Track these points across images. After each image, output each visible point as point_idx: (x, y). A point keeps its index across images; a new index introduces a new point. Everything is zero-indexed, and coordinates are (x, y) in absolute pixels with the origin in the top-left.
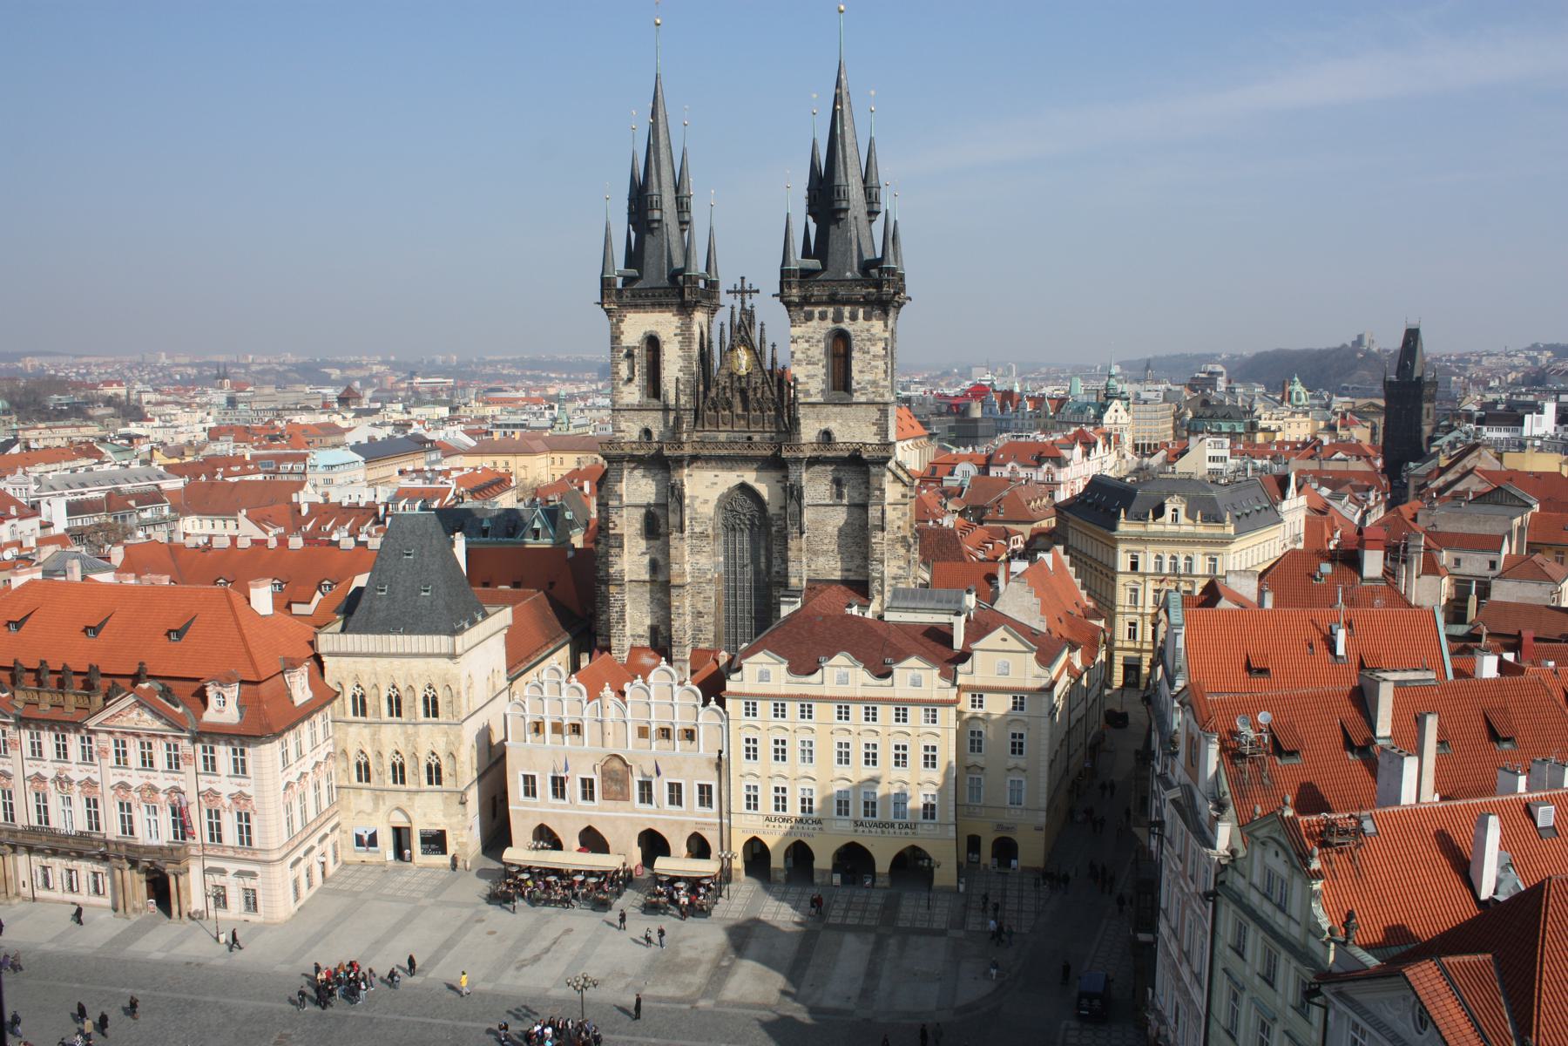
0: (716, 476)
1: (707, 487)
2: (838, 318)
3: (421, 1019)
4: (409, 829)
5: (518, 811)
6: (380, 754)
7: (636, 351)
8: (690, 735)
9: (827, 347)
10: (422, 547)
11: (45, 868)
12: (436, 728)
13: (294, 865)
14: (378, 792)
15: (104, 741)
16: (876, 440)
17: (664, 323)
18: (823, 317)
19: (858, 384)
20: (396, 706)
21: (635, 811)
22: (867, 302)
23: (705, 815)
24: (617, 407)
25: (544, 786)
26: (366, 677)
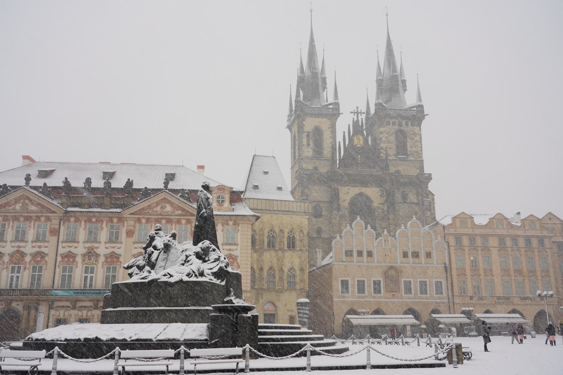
0: (349, 189)
1: (345, 194)
2: (400, 125)
6: (261, 269)
7: (311, 134)
17: (324, 123)
18: (394, 124)
19: (410, 152)
23: (440, 298)
24: (301, 157)
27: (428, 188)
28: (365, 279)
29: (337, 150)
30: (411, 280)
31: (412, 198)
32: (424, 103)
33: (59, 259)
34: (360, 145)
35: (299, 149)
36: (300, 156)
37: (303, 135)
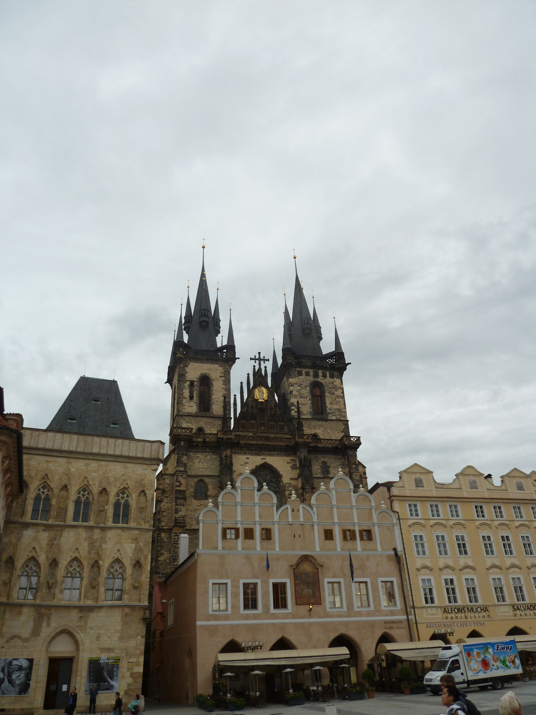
0: (248, 458)
1: (241, 465)
2: (316, 375)
5: (205, 627)
6: (54, 563)
7: (195, 383)
9: (311, 390)
10: (108, 399)
12: (125, 535)
14: (43, 611)
18: (307, 374)
19: (330, 410)
21: (327, 615)
23: (392, 613)
24: (180, 414)
26: (57, 477)
27: (356, 456)
28: (258, 581)
29: (232, 406)
32: (344, 350)
34: (264, 399)
35: (178, 403)
36: (178, 411)
37: (185, 384)
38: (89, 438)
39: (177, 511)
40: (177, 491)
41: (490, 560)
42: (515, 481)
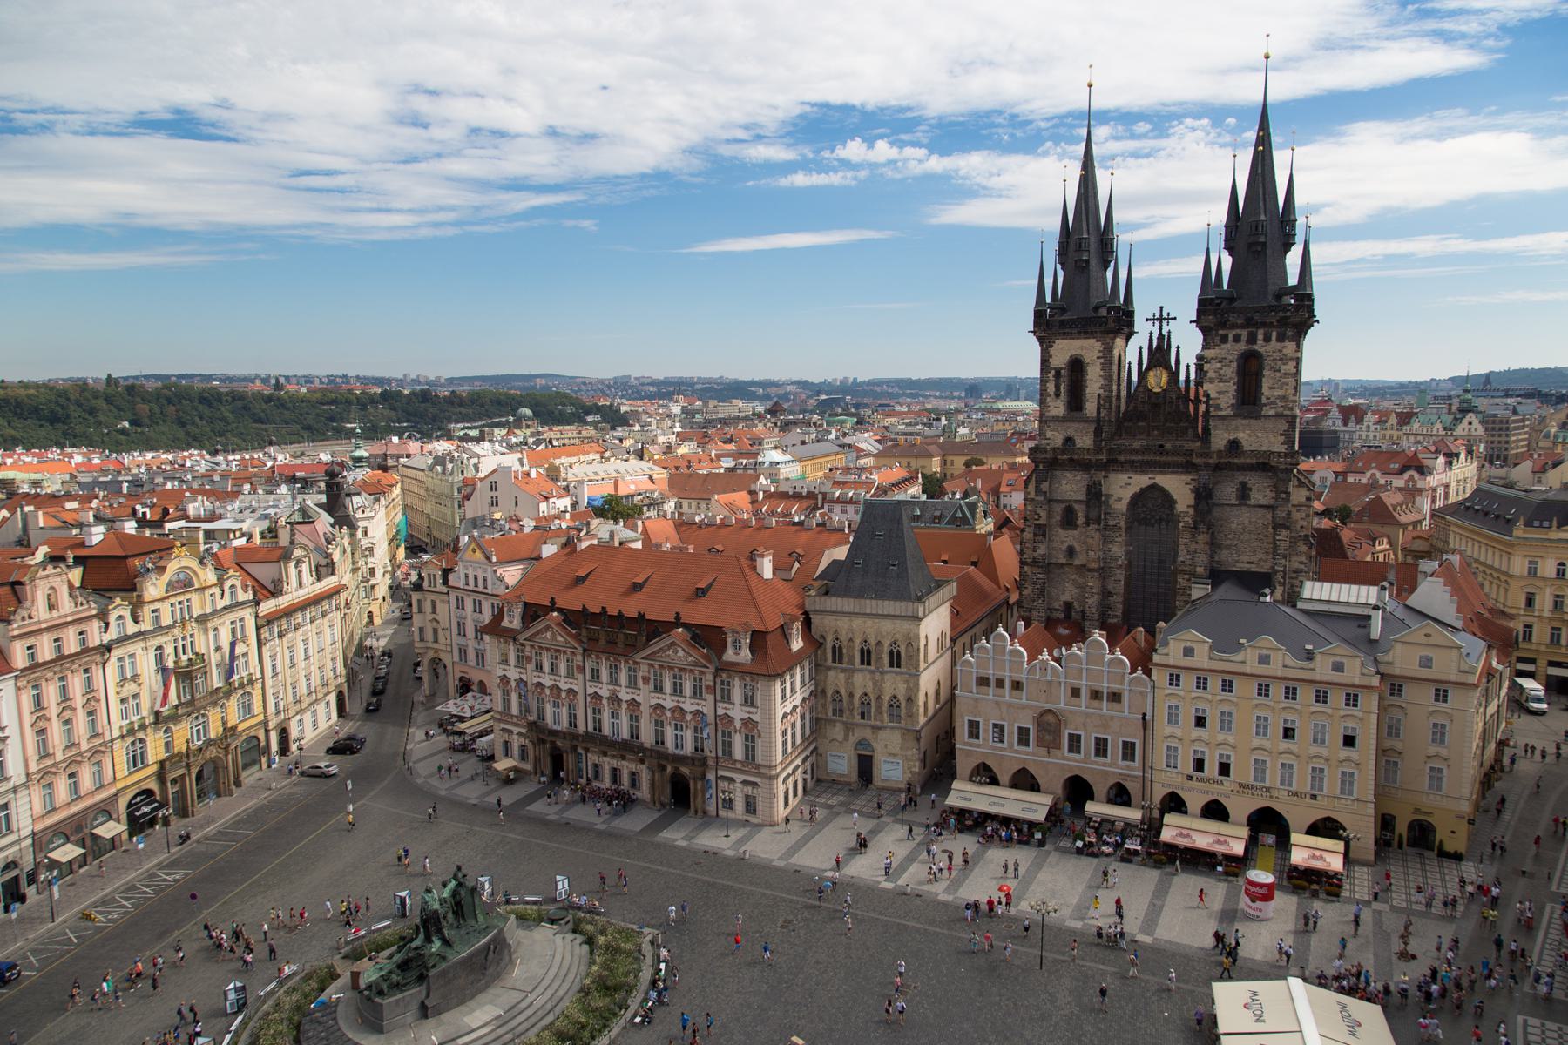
3: (897, 921)
4: (871, 757)
6: (851, 695)
8: (1115, 697)
11: (596, 766)
12: (899, 678)
13: (785, 781)
15: (643, 670)
16: (1283, 449)
17: (1088, 348)
18: (1237, 339)
20: (866, 656)
21: (1064, 758)
22: (1283, 323)
23: (1128, 768)
25: (986, 731)
30: (1082, 733)
31: (1261, 492)
33: (589, 699)
38: (863, 601)
39: (1035, 550)
40: (1039, 526)
41: (1256, 742)
42: (1332, 659)
